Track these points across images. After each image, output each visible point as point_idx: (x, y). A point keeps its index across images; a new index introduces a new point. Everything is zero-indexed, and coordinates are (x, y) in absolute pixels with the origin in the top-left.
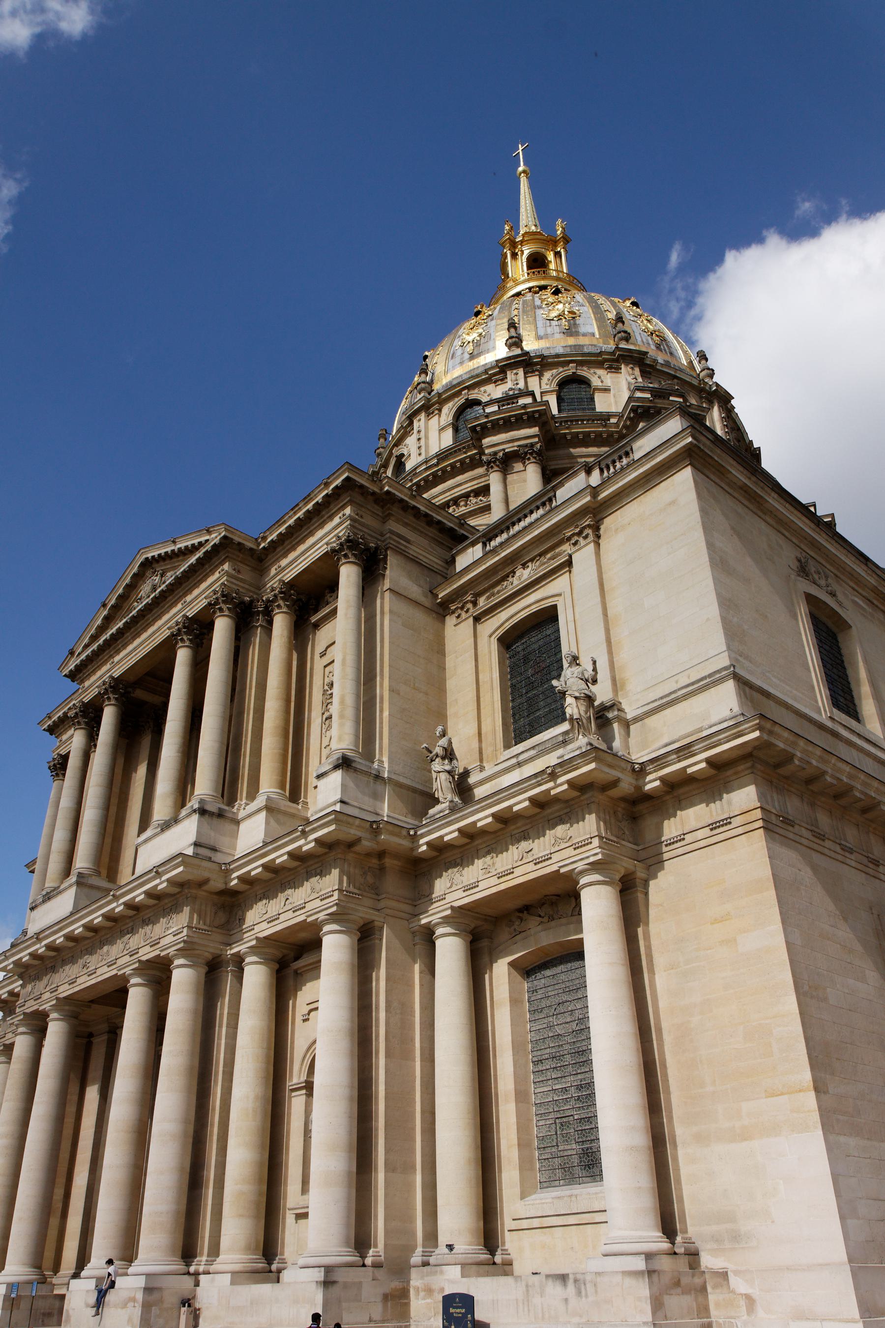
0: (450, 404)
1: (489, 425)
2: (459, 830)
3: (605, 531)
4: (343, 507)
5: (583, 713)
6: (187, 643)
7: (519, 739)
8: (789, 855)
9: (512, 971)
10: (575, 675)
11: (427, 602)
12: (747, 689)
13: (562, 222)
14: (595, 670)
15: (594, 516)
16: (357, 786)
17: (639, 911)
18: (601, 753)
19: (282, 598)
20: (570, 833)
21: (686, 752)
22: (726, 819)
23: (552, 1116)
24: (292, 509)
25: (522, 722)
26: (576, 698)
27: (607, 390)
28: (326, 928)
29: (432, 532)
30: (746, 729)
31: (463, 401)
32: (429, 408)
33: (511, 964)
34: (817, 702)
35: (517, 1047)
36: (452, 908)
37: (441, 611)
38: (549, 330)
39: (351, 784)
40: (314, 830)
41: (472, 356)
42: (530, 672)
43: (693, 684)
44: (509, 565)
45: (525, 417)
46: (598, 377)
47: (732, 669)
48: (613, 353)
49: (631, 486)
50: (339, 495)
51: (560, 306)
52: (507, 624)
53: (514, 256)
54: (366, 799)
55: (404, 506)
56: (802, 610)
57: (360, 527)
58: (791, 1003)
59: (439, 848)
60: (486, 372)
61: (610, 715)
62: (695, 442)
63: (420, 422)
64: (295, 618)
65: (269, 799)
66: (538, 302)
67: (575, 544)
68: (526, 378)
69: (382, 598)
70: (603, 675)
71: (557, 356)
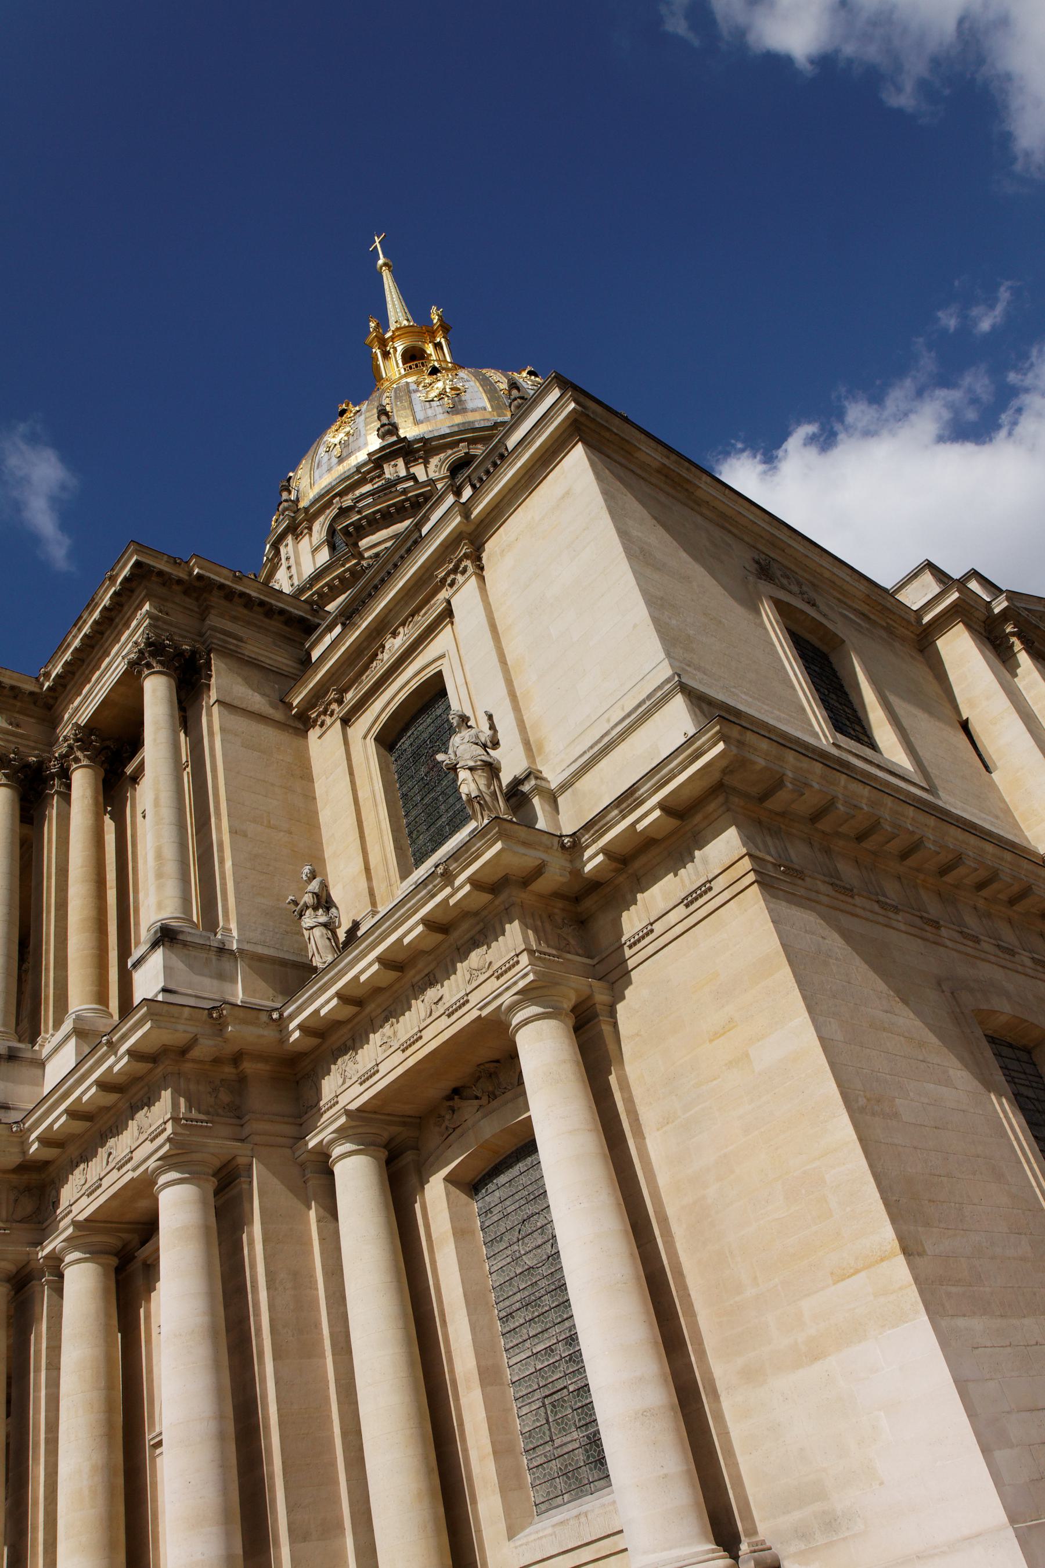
0: (322, 519)
1: (364, 522)
2: (338, 995)
3: (488, 559)
4: (140, 607)
5: (483, 788)
7: (419, 861)
9: (452, 1189)
10: (466, 740)
11: (278, 715)
12: (705, 706)
13: (438, 309)
14: (492, 727)
15: (472, 542)
16: (190, 967)
17: (607, 1051)
18: (508, 826)
19: (80, 748)
21: (629, 802)
22: (704, 884)
23: (538, 1395)
24: (75, 625)
25: (421, 840)
26: (471, 769)
28: (162, 1180)
29: (275, 625)
30: (704, 744)
31: (336, 511)
32: (294, 530)
33: (448, 1179)
34: (811, 725)
35: (473, 1301)
36: (348, 1113)
37: (301, 726)
38: (430, 412)
39: (179, 965)
40: (124, 1038)
41: (341, 459)
42: (423, 770)
43: (629, 715)
44: (375, 639)
45: (407, 504)
47: (676, 678)
49: (510, 490)
50: (132, 591)
51: (440, 385)
52: (383, 715)
53: (386, 355)
54: (207, 981)
55: (229, 594)
56: (768, 614)
57: (165, 627)
58: (842, 1128)
59: (314, 1030)
61: (526, 788)
62: (578, 408)
63: (287, 548)
64: (102, 773)
65: (78, 1019)
67: (452, 585)
69: (210, 715)
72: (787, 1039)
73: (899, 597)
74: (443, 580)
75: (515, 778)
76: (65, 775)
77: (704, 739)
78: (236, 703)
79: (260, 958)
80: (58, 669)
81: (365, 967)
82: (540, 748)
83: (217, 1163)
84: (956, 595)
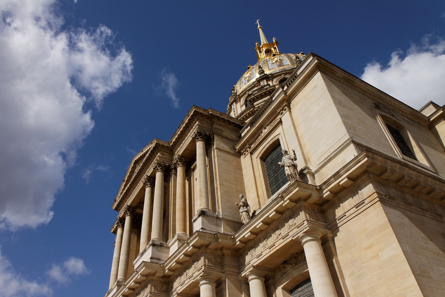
0: (243, 98)
1: (255, 98)
2: (250, 231)
4: (195, 123)
5: (292, 172)
6: (149, 185)
7: (273, 194)
8: (396, 213)
9: (284, 291)
11: (232, 152)
12: (360, 147)
14: (295, 154)
15: (287, 102)
16: (209, 222)
17: (332, 252)
18: (300, 183)
19: (179, 161)
20: (295, 222)
22: (362, 201)
26: (289, 166)
28: (201, 283)
29: (231, 127)
30: (361, 158)
32: (236, 101)
33: (283, 288)
34: (395, 153)
36: (253, 266)
38: (273, 67)
39: (205, 221)
40: (191, 241)
41: (248, 81)
42: (274, 167)
43: (336, 150)
50: (193, 118)
51: (276, 59)
53: (260, 52)
54: (213, 226)
55: (219, 119)
56: (379, 119)
58: (412, 280)
59: (245, 242)
61: (305, 172)
65: (179, 236)
67: (281, 114)
69: (214, 152)
72: (391, 250)
73: (422, 113)
74: (279, 113)
75: (302, 169)
76: (176, 169)
77: (361, 157)
78: (221, 148)
79: (228, 220)
80: (174, 140)
81: (258, 224)
82: (309, 161)
83: (216, 279)
84: (442, 112)
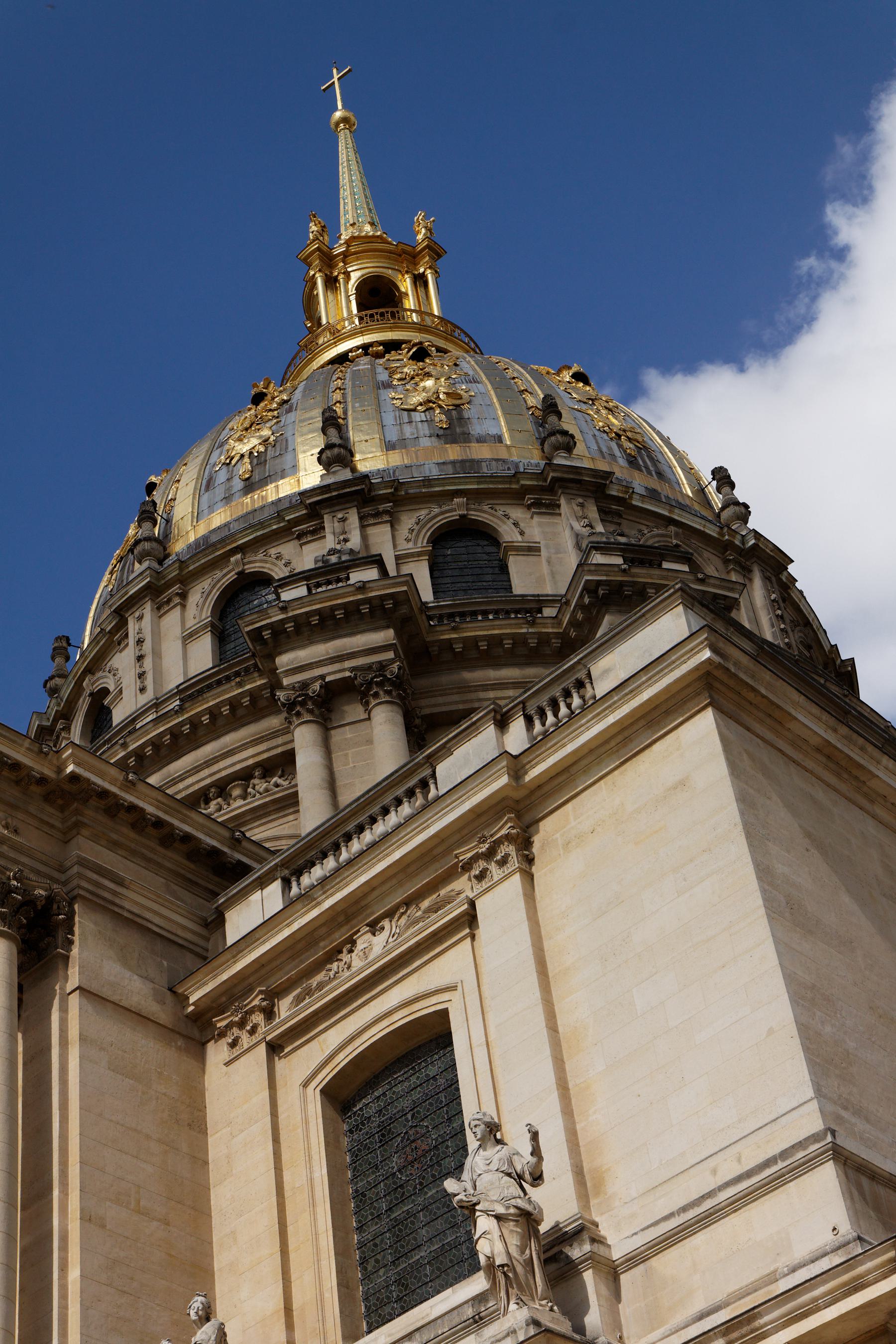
0: (205, 584)
3: (543, 847)
10: (494, 1166)
11: (162, 1013)
12: (865, 1181)
13: (426, 217)
14: (536, 1152)
15: (519, 816)
21: (744, 1330)
25: (381, 1277)
26: (499, 1218)
27: (532, 550)
29: (173, 858)
30: (869, 1272)
31: (232, 576)
32: (162, 591)
37: (196, 1034)
38: (408, 431)
41: (250, 486)
42: (396, 1161)
43: (749, 1174)
44: (340, 925)
45: (365, 609)
46: (513, 524)
47: (829, 1138)
48: (541, 475)
49: (591, 751)
51: (429, 383)
52: (341, 1056)
53: (331, 283)
55: (113, 808)
57: (12, 854)
60: (279, 516)
61: (576, 1252)
62: (717, 659)
63: (143, 622)
66: (383, 376)
67: (481, 877)
68: (363, 527)
69: (64, 1010)
70: (556, 1162)
71: (427, 482)
77: (869, 1265)
78: (106, 992)
